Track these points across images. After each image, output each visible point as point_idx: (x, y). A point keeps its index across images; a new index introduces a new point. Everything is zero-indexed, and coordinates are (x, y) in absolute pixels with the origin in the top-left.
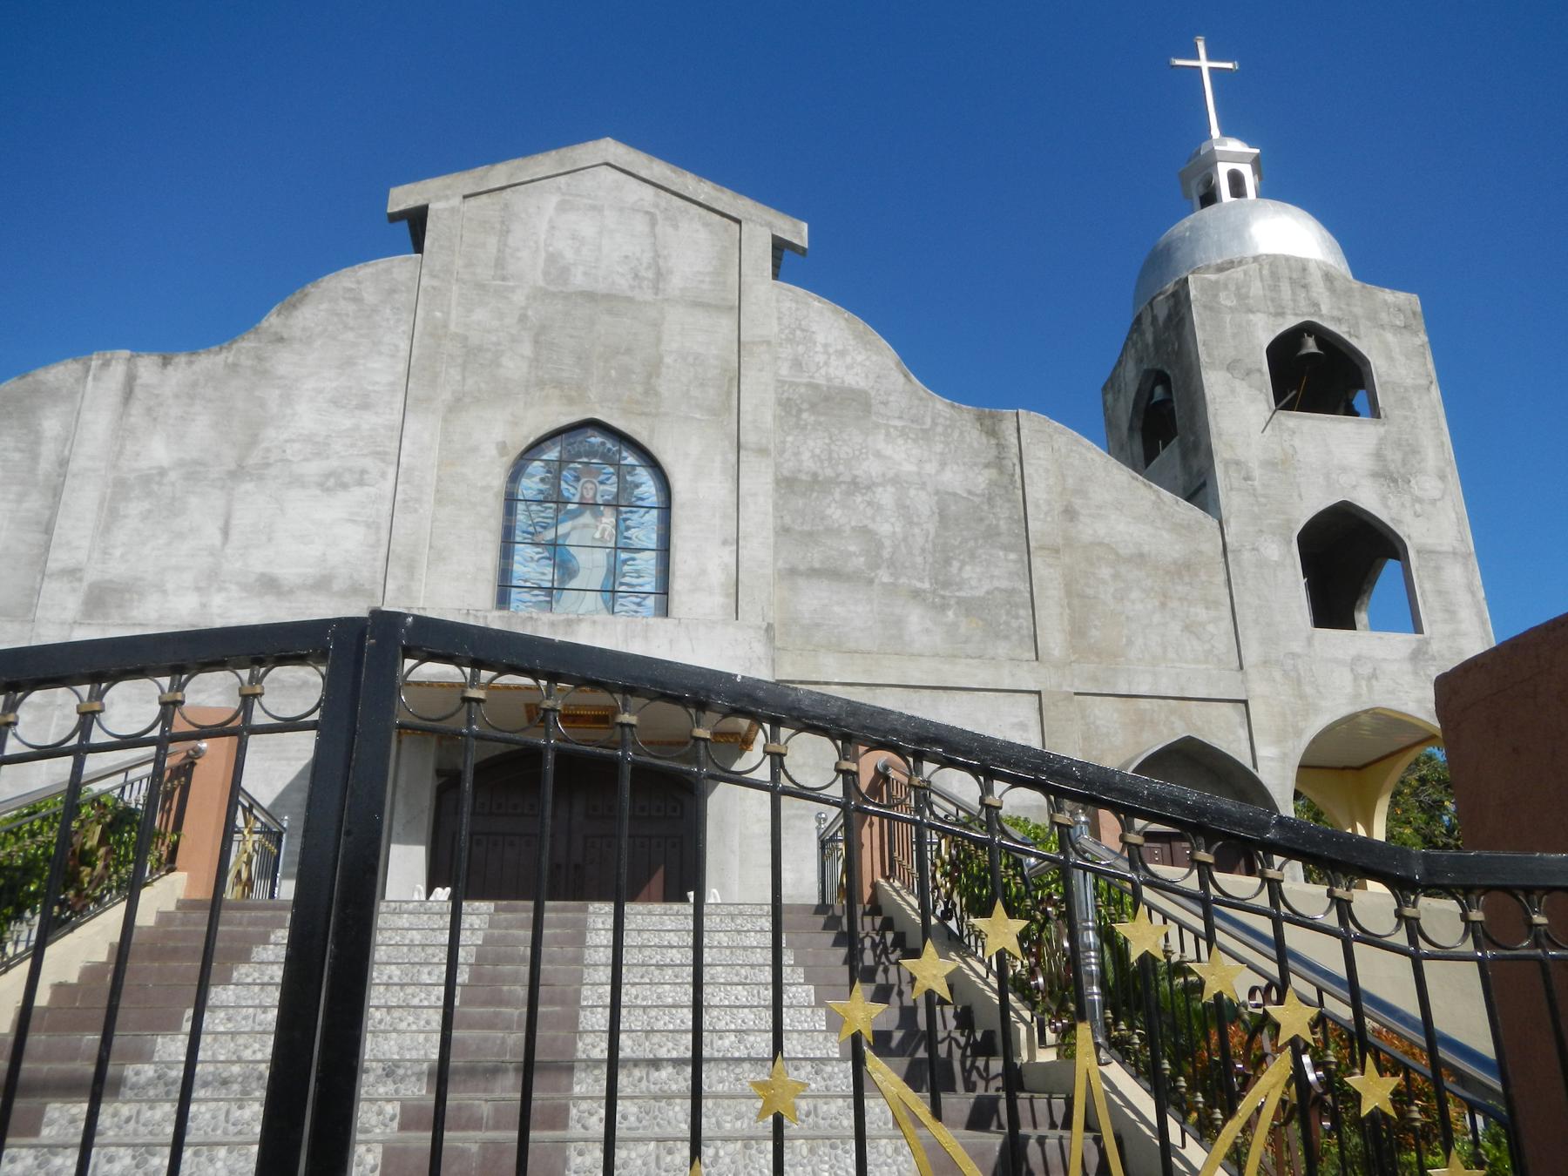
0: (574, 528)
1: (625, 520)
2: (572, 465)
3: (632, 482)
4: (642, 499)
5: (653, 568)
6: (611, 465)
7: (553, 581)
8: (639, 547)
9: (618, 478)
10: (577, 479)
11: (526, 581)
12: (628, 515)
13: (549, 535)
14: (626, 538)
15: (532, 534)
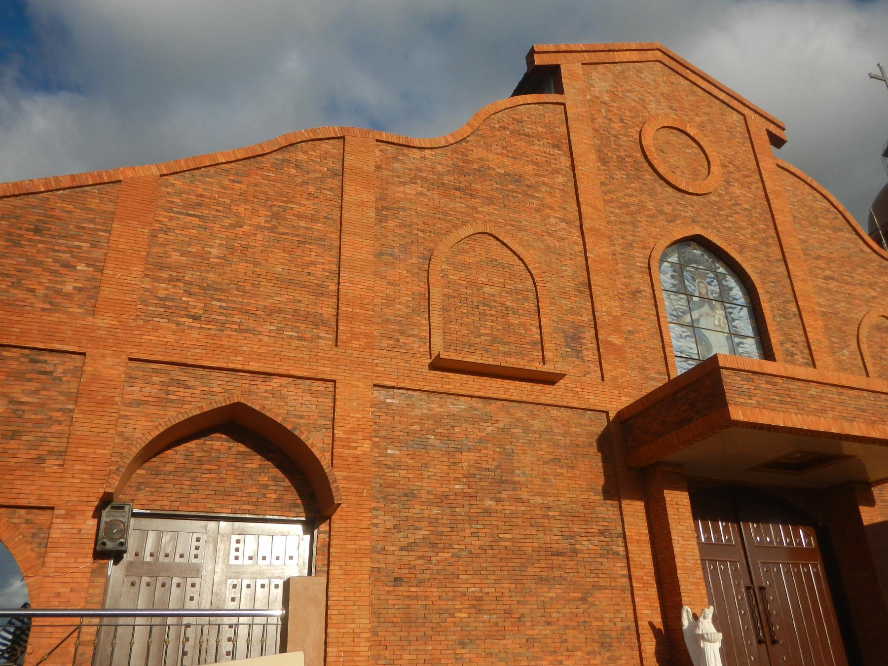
0: (701, 316)
1: (731, 313)
2: (688, 268)
3: (727, 286)
4: (737, 300)
5: (756, 351)
6: (711, 271)
7: (698, 354)
8: (743, 334)
9: (718, 281)
10: (694, 279)
11: (681, 352)
12: (730, 310)
13: (687, 319)
14: (734, 327)
15: (677, 317)
